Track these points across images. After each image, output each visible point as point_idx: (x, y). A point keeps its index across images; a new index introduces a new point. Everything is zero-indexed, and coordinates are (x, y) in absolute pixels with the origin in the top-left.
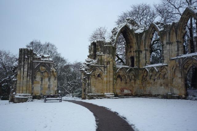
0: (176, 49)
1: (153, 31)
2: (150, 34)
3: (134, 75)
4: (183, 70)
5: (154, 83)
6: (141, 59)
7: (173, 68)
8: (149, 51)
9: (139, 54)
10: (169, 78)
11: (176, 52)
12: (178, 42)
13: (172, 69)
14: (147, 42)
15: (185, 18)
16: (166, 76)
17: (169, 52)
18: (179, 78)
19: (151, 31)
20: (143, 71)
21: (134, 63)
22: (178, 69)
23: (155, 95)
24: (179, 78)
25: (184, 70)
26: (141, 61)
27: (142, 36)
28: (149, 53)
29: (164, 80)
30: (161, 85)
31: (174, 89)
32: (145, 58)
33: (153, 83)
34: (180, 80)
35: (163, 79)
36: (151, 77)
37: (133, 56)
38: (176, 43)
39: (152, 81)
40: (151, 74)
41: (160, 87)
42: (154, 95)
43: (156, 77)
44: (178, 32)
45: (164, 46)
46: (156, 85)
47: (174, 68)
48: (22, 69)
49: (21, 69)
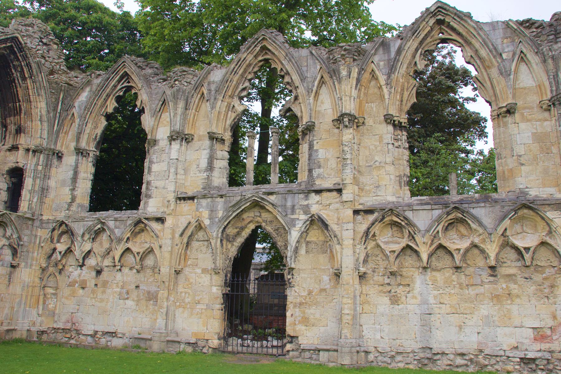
0: (204, 163)
1: (119, 87)
2: (108, 96)
3: (10, 246)
4: (221, 240)
5: (96, 285)
6: (52, 183)
7: (184, 230)
8: (90, 159)
9: (48, 166)
10: (165, 270)
11: (200, 172)
12: (212, 137)
13: (182, 235)
14: (89, 125)
15: (249, 65)
16: (149, 262)
17: (177, 169)
19: (115, 86)
20: (56, 233)
21: (19, 195)
22: (201, 234)
23: (96, 332)
24: (204, 271)
25: (224, 242)
26: (52, 195)
27: (73, 99)
28: (90, 165)
29: (141, 275)
30: (125, 296)
31: (179, 312)
32: (69, 182)
33: (91, 284)
34: (206, 279)
35: (138, 272)
36: (84, 259)
37: (21, 165)
38: (207, 142)
40: (87, 247)
41: (122, 301)
42: (91, 333)
43: (107, 262)
44: (219, 102)
45: (156, 148)
46: (104, 292)
47: (188, 233)
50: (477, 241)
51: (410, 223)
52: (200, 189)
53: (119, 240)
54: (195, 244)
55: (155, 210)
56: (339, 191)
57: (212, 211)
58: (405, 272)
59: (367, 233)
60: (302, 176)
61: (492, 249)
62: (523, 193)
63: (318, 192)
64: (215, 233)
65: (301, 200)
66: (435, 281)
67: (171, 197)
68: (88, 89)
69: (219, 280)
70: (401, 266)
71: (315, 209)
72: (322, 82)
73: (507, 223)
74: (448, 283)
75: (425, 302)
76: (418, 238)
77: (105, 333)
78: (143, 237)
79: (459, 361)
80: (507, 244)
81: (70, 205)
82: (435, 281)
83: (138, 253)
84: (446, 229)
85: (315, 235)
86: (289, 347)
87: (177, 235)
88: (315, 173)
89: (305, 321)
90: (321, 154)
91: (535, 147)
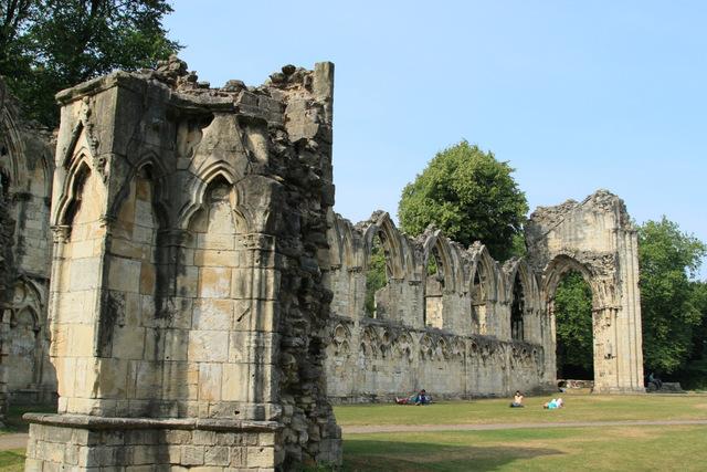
55: (29, 267)
83: (17, 310)
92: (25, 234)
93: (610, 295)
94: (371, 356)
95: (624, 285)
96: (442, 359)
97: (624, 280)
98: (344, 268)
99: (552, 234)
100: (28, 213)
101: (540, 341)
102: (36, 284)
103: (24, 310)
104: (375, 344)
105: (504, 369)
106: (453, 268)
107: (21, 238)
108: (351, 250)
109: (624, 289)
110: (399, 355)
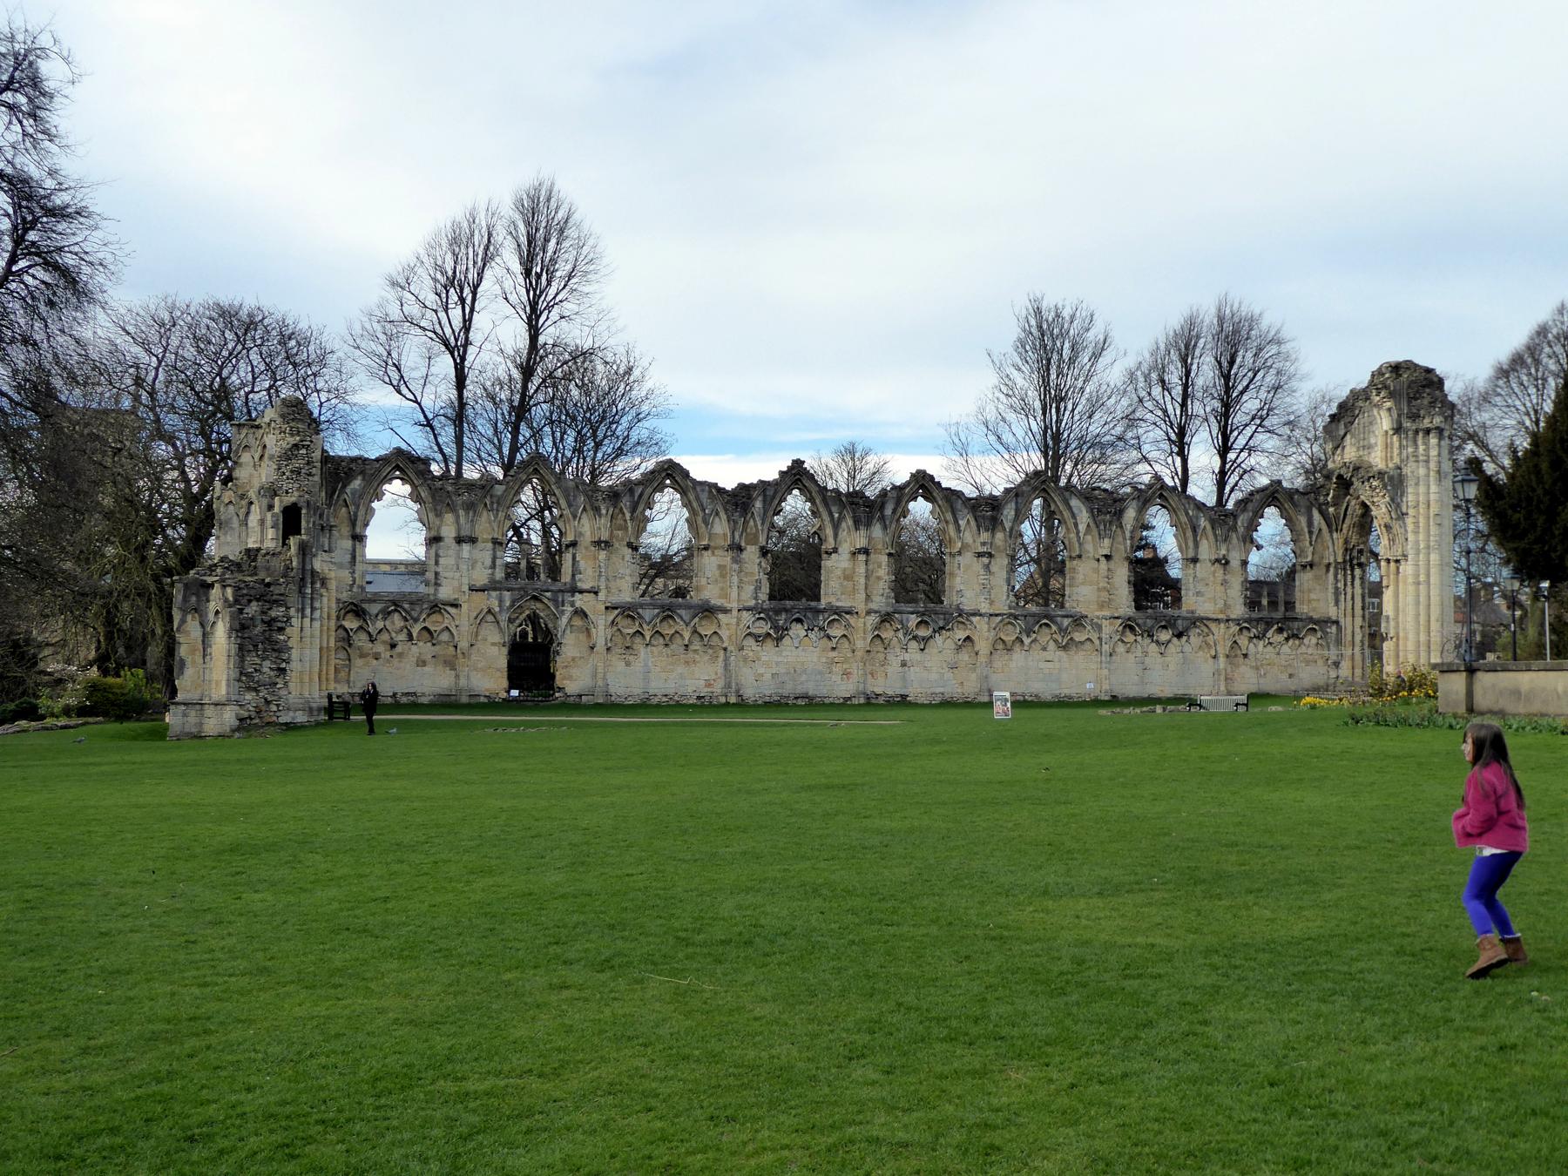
0: (488, 562)
18: (493, 644)
23: (395, 694)
24: (493, 644)
27: (344, 486)
29: (437, 647)
30: (422, 663)
38: (490, 545)
39: (379, 648)
40: (380, 624)
48: (308, 611)
49: (303, 609)
50: (677, 628)
51: (641, 617)
52: (486, 581)
53: (416, 620)
54: (484, 625)
56: (596, 593)
57: (501, 601)
58: (635, 646)
59: (613, 622)
60: (566, 577)
61: (687, 635)
62: (707, 602)
63: (581, 592)
64: (503, 618)
65: (568, 597)
66: (652, 652)
67: (466, 588)
68: (360, 478)
69: (505, 651)
70: (633, 643)
71: (578, 604)
72: (584, 509)
73: (697, 619)
74: (660, 653)
75: (646, 665)
76: (645, 626)
77: (407, 694)
78: (435, 617)
79: (665, 699)
80: (695, 632)
81: (352, 586)
82: (652, 652)
84: (661, 621)
85: (578, 622)
86: (557, 695)
87: (472, 618)
88: (578, 577)
89: (570, 678)
90: (582, 564)
91: (717, 573)
92: (439, 569)
93: (1386, 537)
94: (898, 650)
95: (1409, 521)
96: (1052, 645)
97: (1411, 512)
98: (845, 549)
99: (1348, 436)
100: (441, 553)
101: (1332, 612)
102: (449, 609)
103: (443, 630)
104: (900, 634)
105: (1215, 657)
106: (1076, 525)
107: (437, 574)
108: (852, 528)
109: (1410, 527)
110: (954, 646)
